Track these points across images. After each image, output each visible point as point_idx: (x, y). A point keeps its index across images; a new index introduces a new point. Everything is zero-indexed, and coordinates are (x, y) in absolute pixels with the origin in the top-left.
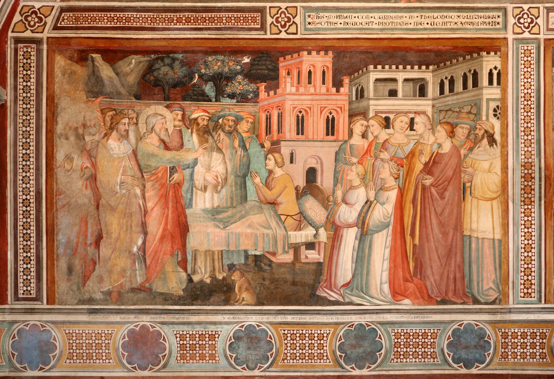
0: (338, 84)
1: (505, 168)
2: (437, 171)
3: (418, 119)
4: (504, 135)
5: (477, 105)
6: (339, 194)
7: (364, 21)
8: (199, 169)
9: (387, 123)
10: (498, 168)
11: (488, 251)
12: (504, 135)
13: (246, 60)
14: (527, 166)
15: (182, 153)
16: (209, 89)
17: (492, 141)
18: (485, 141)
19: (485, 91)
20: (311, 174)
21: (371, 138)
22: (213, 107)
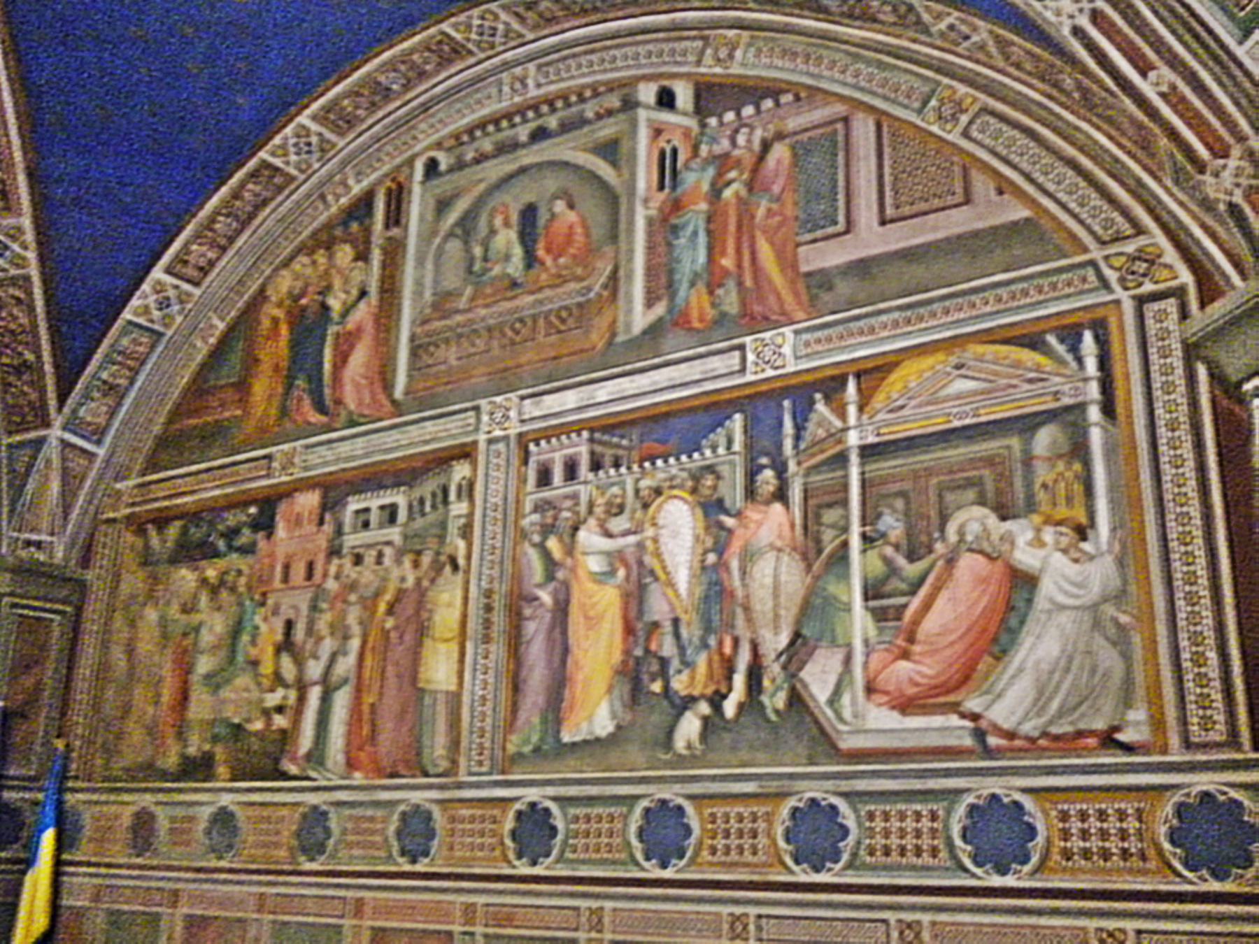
0: (321, 522)
1: (466, 599)
2: (398, 608)
3: (388, 551)
4: (469, 557)
5: (443, 525)
6: (309, 646)
7: (348, 448)
8: (204, 631)
9: (358, 560)
10: (458, 601)
11: (441, 709)
12: (469, 557)
13: (253, 510)
14: (488, 594)
15: (192, 615)
16: (221, 544)
17: (455, 567)
18: (448, 569)
19: (452, 507)
20: (289, 625)
21: (344, 579)
22: (221, 563)
